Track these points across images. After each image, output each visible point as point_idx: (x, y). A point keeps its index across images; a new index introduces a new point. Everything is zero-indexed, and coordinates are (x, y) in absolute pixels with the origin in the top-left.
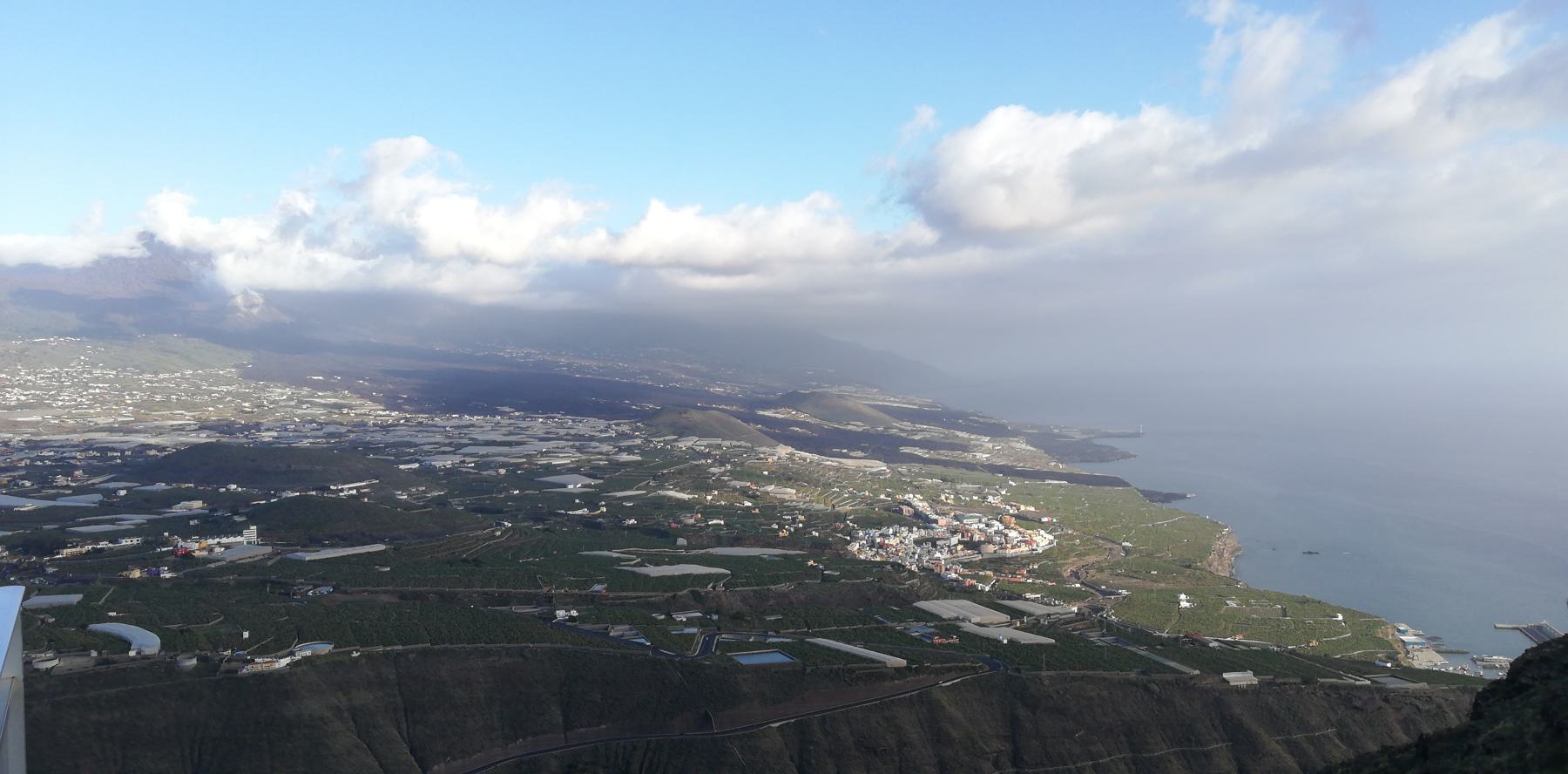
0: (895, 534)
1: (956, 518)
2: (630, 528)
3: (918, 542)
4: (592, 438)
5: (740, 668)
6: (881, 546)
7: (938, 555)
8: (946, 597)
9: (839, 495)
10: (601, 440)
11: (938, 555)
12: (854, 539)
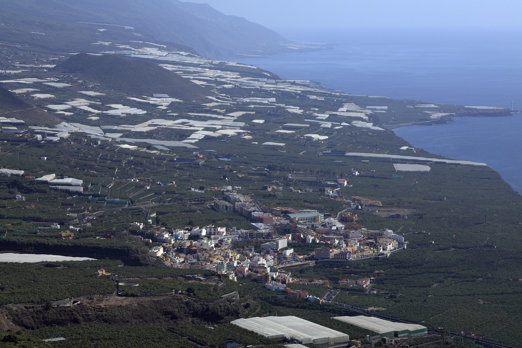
0: (208, 236)
1: (285, 214)
6: (190, 251)
7: (262, 261)
8: (271, 313)
9: (139, 187)
11: (262, 261)
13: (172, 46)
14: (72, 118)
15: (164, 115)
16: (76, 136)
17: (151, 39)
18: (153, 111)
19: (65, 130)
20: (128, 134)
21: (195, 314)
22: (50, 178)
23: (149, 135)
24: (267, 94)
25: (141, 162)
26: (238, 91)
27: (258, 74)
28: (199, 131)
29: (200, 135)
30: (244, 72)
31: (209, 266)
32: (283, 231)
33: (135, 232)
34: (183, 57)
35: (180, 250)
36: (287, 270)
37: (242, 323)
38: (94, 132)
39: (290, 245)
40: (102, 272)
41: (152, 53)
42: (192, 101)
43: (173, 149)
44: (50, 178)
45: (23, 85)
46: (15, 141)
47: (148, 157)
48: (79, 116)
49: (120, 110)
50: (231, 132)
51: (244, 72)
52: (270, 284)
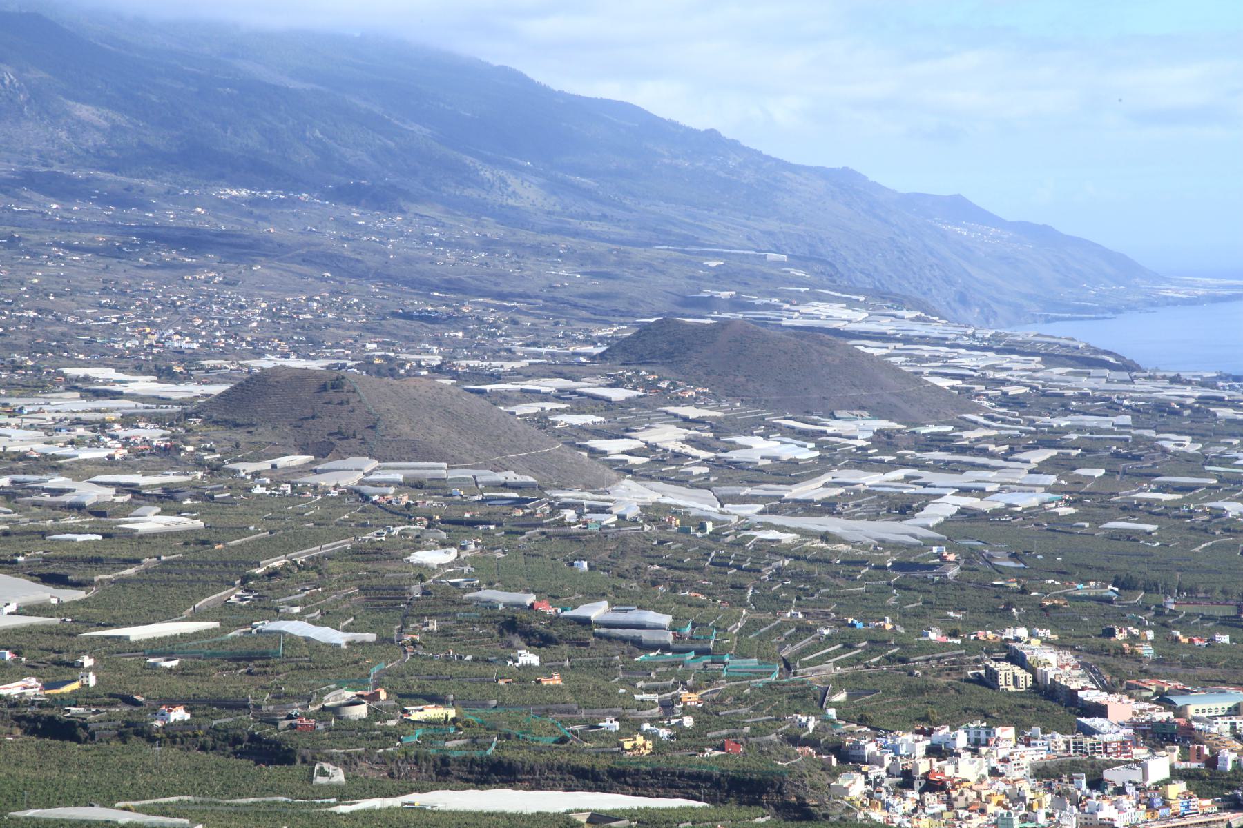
1: (1163, 700)
2: (173, 735)
3: (1042, 773)
4: (50, 464)
6: (932, 785)
9: (804, 630)
10: (80, 471)
12: (850, 758)
14: (647, 471)
15: (860, 460)
16: (654, 513)
19: (630, 497)
20: (779, 506)
23: (828, 507)
27: (1088, 361)
29: (949, 505)
32: (1157, 736)
34: (906, 320)
35: (907, 780)
38: (698, 503)
39: (1176, 774)
42: (924, 426)
44: (597, 611)
45: (535, 396)
48: (660, 466)
49: (759, 448)
50: (1024, 501)
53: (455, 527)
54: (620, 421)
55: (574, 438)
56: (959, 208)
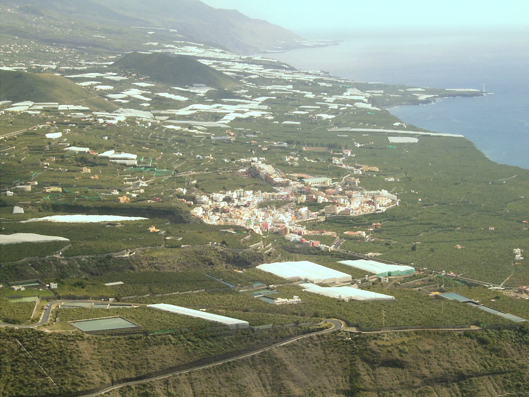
1: (301, 179)
5: (80, 336)
7: (282, 217)
8: (289, 259)
12: (197, 203)
13: (208, 45)
15: (201, 100)
16: (131, 120)
17: (190, 38)
18: (194, 99)
20: (173, 117)
21: (228, 261)
22: (110, 154)
23: (190, 117)
24: (287, 82)
25: (184, 140)
26: (262, 80)
27: (278, 66)
28: (230, 112)
29: (231, 117)
30: (267, 65)
31: (239, 223)
33: (179, 196)
34: (217, 53)
35: (216, 210)
36: (303, 224)
37: (265, 267)
38: (145, 116)
40: (153, 229)
41: (192, 51)
43: (210, 129)
44: (110, 154)
46: (81, 124)
47: (190, 135)
48: (134, 103)
50: (257, 114)
51: (267, 65)
52: (289, 236)
53: (61, 125)
54: (119, 87)
55: (103, 94)
56: (235, 15)
